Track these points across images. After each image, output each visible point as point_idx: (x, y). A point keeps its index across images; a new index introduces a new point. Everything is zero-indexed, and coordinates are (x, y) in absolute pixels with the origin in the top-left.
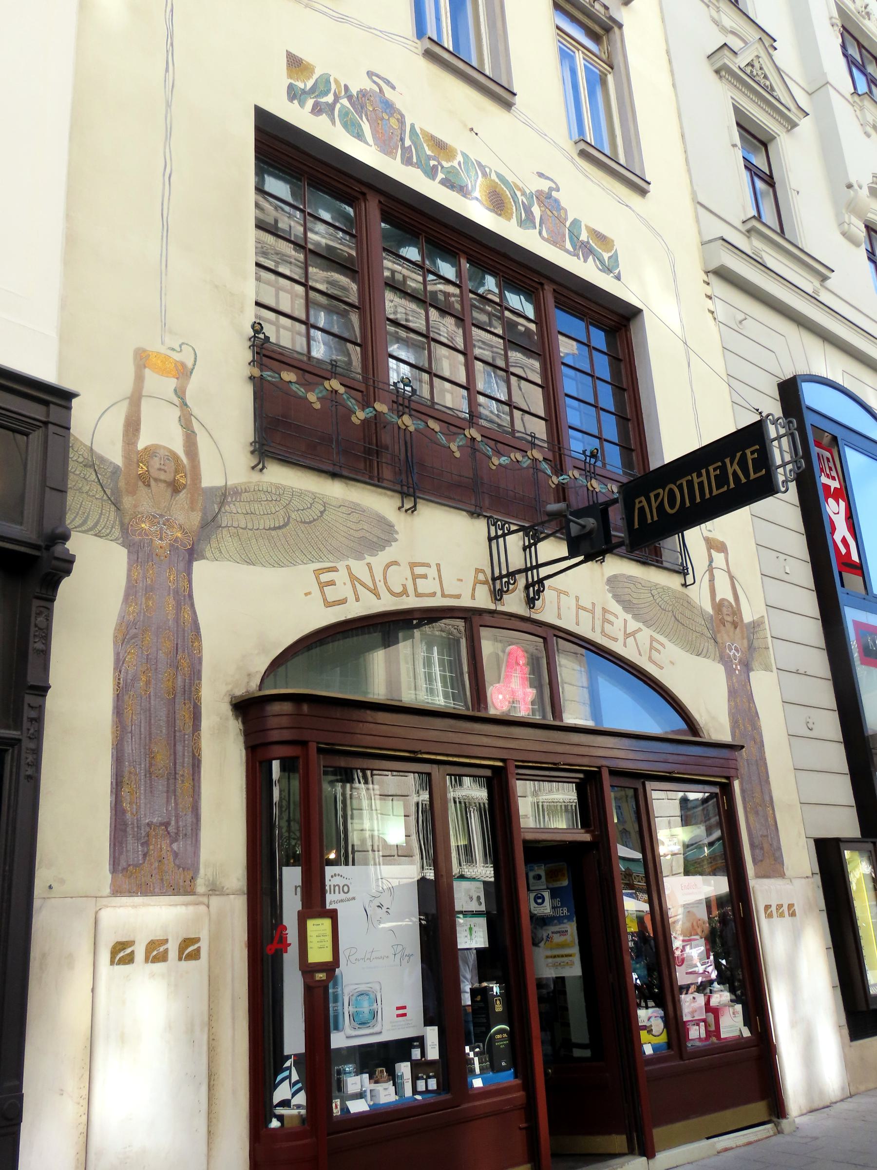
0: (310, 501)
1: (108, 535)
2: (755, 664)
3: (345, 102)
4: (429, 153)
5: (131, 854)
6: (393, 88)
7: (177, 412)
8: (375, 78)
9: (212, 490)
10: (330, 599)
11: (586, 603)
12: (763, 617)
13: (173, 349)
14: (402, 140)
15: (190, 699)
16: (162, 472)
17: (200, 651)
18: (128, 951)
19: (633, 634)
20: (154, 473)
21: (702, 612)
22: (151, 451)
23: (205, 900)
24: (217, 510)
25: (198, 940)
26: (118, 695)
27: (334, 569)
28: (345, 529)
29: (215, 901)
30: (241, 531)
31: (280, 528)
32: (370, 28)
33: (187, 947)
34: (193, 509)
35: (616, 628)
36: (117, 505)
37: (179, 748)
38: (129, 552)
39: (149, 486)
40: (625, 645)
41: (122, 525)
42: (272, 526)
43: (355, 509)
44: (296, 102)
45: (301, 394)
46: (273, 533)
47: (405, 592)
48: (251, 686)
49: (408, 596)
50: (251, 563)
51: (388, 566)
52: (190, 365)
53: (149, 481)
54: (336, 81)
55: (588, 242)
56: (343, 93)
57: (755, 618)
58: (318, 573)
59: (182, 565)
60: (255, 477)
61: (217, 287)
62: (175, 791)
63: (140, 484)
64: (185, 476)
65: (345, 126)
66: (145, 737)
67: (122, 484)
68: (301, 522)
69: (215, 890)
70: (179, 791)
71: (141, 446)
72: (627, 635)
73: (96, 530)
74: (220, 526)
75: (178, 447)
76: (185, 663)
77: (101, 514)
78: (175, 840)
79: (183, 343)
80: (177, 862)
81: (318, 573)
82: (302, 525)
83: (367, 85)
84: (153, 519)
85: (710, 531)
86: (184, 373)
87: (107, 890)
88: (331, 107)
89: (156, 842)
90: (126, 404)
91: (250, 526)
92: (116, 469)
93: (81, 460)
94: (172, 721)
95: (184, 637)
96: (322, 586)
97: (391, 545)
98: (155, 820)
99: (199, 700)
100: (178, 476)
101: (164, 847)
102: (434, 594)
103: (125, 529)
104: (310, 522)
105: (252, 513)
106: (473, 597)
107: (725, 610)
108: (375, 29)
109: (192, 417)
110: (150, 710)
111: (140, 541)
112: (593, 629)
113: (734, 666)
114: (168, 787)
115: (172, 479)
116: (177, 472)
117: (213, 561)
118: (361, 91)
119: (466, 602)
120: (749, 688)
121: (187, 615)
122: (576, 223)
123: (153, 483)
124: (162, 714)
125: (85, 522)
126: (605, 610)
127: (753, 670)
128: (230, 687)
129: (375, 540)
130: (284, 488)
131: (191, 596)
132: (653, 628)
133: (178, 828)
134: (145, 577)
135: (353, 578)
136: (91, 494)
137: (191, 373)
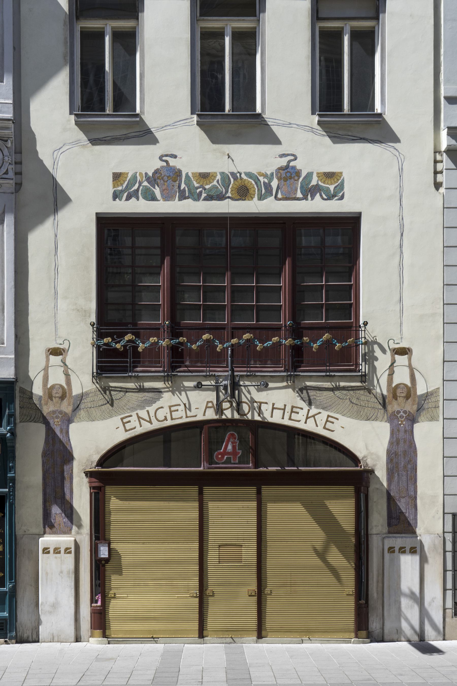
1: (38, 421)
2: (422, 418)
3: (145, 184)
4: (196, 185)
6: (175, 157)
8: (164, 158)
10: (127, 428)
12: (438, 388)
13: (61, 344)
14: (179, 187)
15: (69, 473)
16: (57, 394)
19: (314, 416)
20: (54, 395)
22: (53, 387)
25: (71, 548)
26: (44, 474)
27: (131, 416)
32: (163, 128)
38: (46, 426)
39: (52, 400)
40: (306, 423)
42: (102, 404)
44: (117, 199)
49: (167, 420)
54: (141, 174)
55: (317, 185)
56: (144, 179)
58: (122, 419)
61: (78, 310)
62: (64, 503)
65: (146, 198)
66: (54, 487)
72: (307, 418)
77: (36, 414)
81: (122, 419)
83: (159, 164)
84: (54, 412)
85: (397, 343)
88: (137, 190)
90: (43, 372)
92: (41, 397)
93: (28, 397)
95: (66, 452)
96: (124, 424)
98: (57, 512)
99: (72, 472)
102: (181, 418)
104: (120, 399)
105: (93, 401)
106: (204, 415)
108: (166, 126)
109: (69, 370)
110: (55, 478)
112: (283, 418)
115: (61, 395)
116: (63, 392)
117: (77, 423)
118: (155, 171)
119: (200, 418)
122: (309, 175)
126: (293, 407)
127: (418, 422)
128: (84, 467)
135: (139, 418)
136: (32, 408)
137: (68, 351)
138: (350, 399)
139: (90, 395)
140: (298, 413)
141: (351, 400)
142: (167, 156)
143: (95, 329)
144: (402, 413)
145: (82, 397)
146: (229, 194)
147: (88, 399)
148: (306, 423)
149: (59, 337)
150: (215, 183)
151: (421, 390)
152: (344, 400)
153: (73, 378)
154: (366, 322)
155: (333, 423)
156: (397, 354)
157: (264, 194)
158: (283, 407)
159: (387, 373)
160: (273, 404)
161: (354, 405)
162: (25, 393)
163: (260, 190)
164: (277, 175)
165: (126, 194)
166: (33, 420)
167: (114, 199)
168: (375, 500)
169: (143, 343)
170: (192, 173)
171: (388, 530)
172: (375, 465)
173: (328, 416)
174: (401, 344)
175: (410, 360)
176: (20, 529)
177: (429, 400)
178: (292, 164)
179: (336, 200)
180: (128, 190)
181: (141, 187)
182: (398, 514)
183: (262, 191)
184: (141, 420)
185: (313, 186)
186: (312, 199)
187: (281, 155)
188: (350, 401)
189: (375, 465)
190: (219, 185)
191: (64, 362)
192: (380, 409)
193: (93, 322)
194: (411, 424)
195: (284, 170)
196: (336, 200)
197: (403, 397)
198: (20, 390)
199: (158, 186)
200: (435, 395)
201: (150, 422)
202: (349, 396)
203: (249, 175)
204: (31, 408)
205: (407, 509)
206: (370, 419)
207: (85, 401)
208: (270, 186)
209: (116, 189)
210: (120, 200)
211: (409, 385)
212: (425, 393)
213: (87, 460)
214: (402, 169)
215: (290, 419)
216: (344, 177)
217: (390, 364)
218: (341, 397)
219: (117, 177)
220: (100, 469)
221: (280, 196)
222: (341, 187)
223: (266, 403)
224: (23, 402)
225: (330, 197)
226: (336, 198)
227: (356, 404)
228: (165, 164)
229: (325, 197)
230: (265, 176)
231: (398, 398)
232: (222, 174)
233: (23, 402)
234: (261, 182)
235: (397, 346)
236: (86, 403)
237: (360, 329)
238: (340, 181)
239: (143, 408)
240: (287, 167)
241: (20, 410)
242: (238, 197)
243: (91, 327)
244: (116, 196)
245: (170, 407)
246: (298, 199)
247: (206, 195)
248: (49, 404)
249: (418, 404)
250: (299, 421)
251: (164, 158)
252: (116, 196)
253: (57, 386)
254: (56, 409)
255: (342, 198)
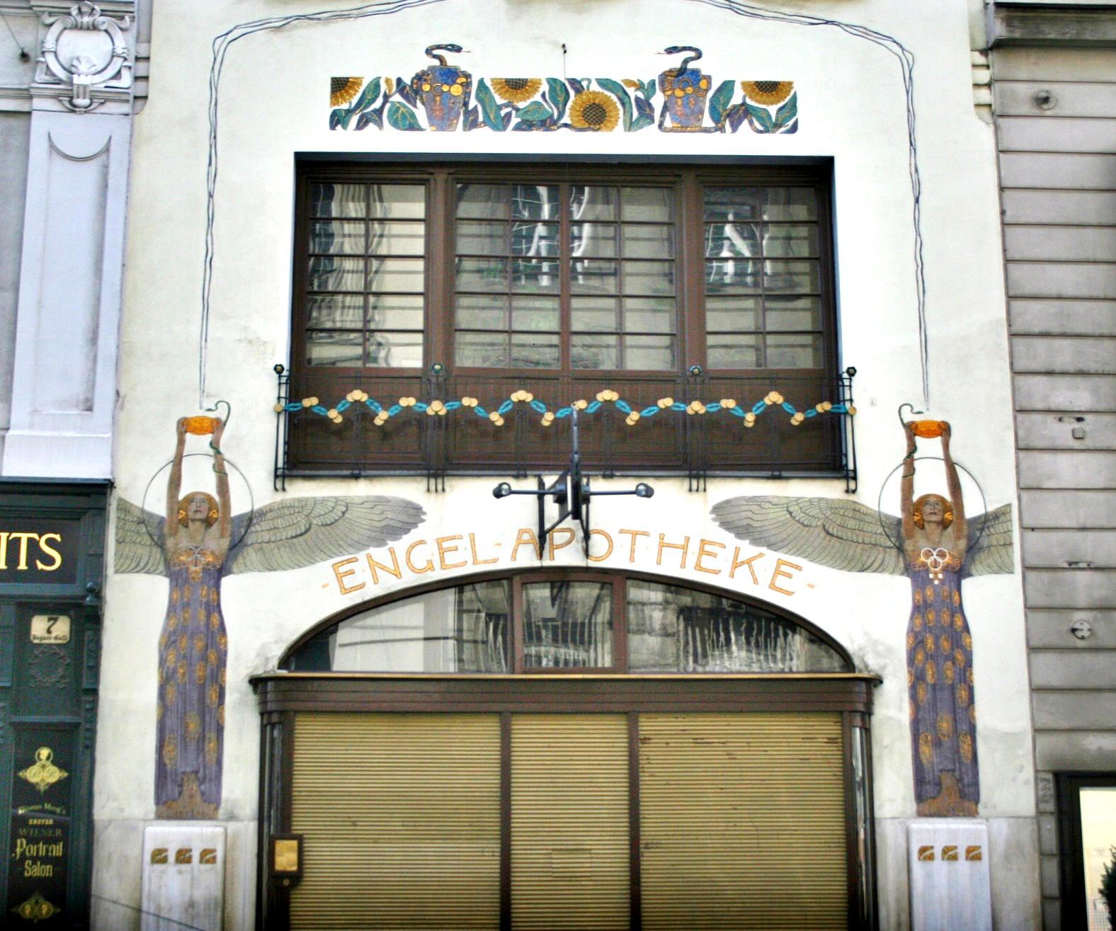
0: (332, 504)
3: (397, 98)
5: (169, 792)
6: (456, 49)
7: (211, 461)
8: (436, 52)
9: (240, 517)
11: (675, 538)
12: (1009, 505)
13: (210, 410)
14: (466, 104)
17: (226, 644)
18: (164, 855)
19: (749, 562)
20: (191, 515)
21: (882, 519)
22: (190, 499)
23: (224, 824)
24: (243, 533)
27: (357, 560)
28: (367, 522)
29: (232, 826)
30: (264, 545)
31: (301, 535)
33: (206, 855)
34: (222, 536)
35: (722, 561)
36: (162, 546)
37: (207, 718)
38: (171, 581)
39: (187, 526)
40: (732, 576)
41: (166, 560)
43: (381, 501)
44: (339, 127)
45: (322, 414)
46: (295, 541)
47: (432, 568)
48: (271, 667)
50: (271, 569)
51: (413, 547)
52: (224, 418)
53: (187, 523)
54: (388, 81)
56: (394, 88)
57: (991, 509)
59: (212, 582)
60: (280, 497)
61: (250, 342)
63: (180, 526)
64: (218, 511)
65: (395, 124)
67: (166, 530)
68: (323, 525)
69: (232, 817)
70: (206, 749)
71: (181, 496)
72: (736, 565)
73: (145, 570)
74: (246, 545)
75: (211, 489)
76: (212, 657)
78: (202, 782)
79: (219, 402)
80: (204, 798)
82: (323, 529)
84: (189, 551)
85: (919, 413)
86: (217, 426)
87: (152, 816)
88: (379, 112)
89: (189, 785)
90: (170, 466)
91: (273, 539)
92: (162, 519)
93: (135, 519)
94: (202, 699)
96: (339, 577)
97: (417, 527)
99: (224, 682)
100: (211, 513)
101: (195, 788)
103: (167, 564)
104: (332, 524)
106: (514, 558)
107: (928, 509)
109: (225, 463)
110: (185, 693)
111: (180, 570)
112: (683, 565)
113: (931, 576)
114: (198, 746)
116: (210, 510)
118: (417, 75)
119: (505, 564)
120: (956, 597)
121: (215, 620)
122: (727, 87)
123: (190, 524)
124: (195, 695)
125: (138, 565)
126: (703, 542)
127: (970, 575)
129: (400, 525)
130: (307, 499)
131: (219, 605)
132: (785, 550)
133: (205, 773)
134: (182, 597)
135: (373, 565)
137: (225, 424)
138: (824, 526)
139: (269, 516)
140: (715, 555)
141: (827, 528)
142: (439, 47)
143: (284, 380)
144: (935, 556)
145: (250, 520)
146: (566, 119)
147: (265, 525)
148: (732, 576)
149: (208, 396)
150: (537, 97)
151: (973, 507)
152: (812, 529)
153: (234, 480)
154: (853, 368)
155: (790, 576)
156: (920, 435)
157: (636, 120)
158: (682, 542)
159: (901, 471)
160: (662, 537)
161: (834, 540)
162: (129, 512)
163: (628, 112)
164: (662, 83)
165: (354, 119)
166: (142, 569)
167: (333, 126)
168: (886, 741)
169: (386, 409)
170: (492, 80)
171: (918, 808)
172: (884, 667)
173: (780, 562)
174: (926, 413)
175: (946, 446)
176: (103, 807)
177: (992, 530)
178: (691, 65)
179: (782, 133)
180: (361, 110)
181: (388, 106)
182: (936, 773)
183: (632, 115)
184: (379, 571)
185: (735, 107)
186: (734, 129)
187: (670, 48)
188: (825, 529)
189: (884, 667)
190: (546, 101)
191: (215, 445)
192: (890, 548)
193: (281, 365)
194: (956, 579)
195: (677, 76)
196: (782, 133)
197: (934, 522)
198: (119, 505)
199: (423, 103)
200: (1002, 518)
201: (398, 575)
202: (822, 521)
203: (604, 83)
204: (140, 543)
205: (954, 762)
206: (867, 568)
207: (258, 528)
208: (650, 105)
209: (336, 107)
210: (345, 127)
211: (948, 497)
212: (982, 515)
213: (258, 655)
214: (910, 78)
215: (699, 567)
216: (795, 94)
217: (904, 454)
218: (805, 523)
219: (340, 86)
220: (284, 673)
221: (668, 123)
222: (792, 107)
223: (645, 534)
224: (124, 529)
225: (770, 127)
226: (783, 129)
227: (837, 537)
228: (436, 63)
229: (761, 128)
230: (640, 86)
231: (926, 525)
232: (553, 82)
233: (124, 529)
234: (629, 97)
235: (917, 418)
236: (259, 533)
237: (841, 383)
238: (789, 98)
239: (380, 542)
240: (682, 71)
241: (116, 546)
242: (587, 125)
243: (277, 376)
244: (337, 120)
245: (439, 542)
246: (707, 130)
247: (519, 120)
248: (179, 534)
249: (969, 538)
250: (717, 572)
251: (436, 52)
252: (337, 120)
253: (199, 497)
254: (195, 545)
255: (794, 129)
